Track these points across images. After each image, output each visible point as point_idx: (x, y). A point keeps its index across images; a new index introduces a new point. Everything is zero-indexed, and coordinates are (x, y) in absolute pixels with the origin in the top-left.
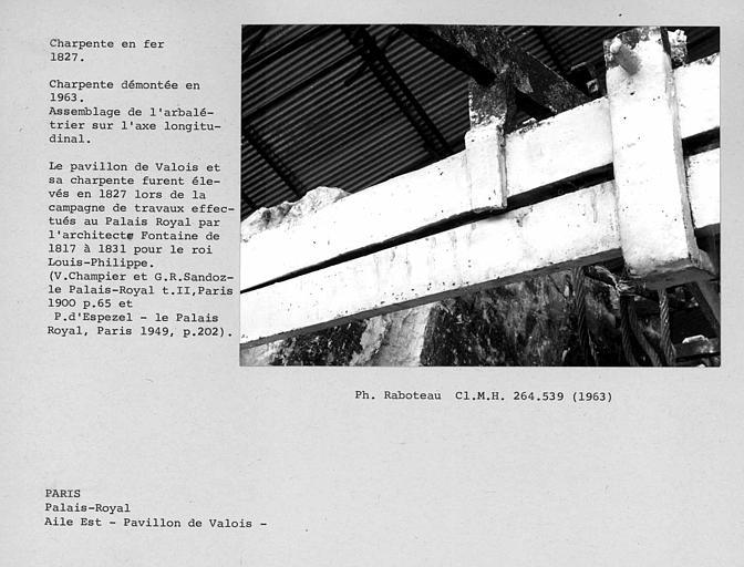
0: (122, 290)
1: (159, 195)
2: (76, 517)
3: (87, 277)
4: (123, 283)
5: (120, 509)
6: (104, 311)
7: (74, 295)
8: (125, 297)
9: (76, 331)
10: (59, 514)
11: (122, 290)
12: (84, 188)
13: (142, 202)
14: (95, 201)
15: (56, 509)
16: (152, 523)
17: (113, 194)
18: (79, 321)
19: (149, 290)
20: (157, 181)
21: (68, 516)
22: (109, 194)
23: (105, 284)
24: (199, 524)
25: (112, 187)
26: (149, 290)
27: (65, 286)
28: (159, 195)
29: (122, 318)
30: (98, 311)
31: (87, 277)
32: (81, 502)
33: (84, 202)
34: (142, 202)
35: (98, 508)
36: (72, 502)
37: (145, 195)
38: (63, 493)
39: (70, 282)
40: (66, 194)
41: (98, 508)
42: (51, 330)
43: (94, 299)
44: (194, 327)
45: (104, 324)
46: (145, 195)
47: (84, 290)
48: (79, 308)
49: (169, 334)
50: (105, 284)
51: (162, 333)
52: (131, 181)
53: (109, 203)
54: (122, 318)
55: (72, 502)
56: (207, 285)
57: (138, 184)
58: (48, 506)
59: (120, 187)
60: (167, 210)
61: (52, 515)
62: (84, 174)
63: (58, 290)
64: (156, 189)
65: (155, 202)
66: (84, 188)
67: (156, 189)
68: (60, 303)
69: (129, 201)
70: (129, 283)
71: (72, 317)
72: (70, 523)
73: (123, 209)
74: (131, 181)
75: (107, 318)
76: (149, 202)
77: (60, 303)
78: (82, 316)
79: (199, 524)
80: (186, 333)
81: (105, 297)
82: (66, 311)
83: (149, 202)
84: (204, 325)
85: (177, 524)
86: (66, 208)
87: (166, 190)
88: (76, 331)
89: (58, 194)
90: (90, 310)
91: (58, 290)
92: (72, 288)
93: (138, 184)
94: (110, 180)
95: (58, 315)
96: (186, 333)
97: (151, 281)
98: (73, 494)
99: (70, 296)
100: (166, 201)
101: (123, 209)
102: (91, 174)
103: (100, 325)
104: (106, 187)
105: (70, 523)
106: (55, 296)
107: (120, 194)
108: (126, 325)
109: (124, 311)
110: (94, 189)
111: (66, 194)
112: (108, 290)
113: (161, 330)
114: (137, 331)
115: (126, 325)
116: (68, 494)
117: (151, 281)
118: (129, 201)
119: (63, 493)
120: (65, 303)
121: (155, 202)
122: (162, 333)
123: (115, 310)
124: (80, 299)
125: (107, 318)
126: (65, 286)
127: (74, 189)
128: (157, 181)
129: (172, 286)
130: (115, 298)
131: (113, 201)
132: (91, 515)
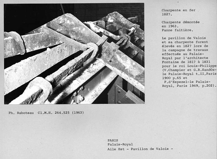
0: (184, 74)
1: (201, 46)
2: (117, 147)
3: (174, 70)
4: (184, 72)
5: (130, 145)
6: (179, 80)
7: (170, 76)
8: (185, 76)
9: (171, 86)
10: (112, 147)
11: (184, 74)
12: (179, 44)
13: (196, 48)
14: (182, 48)
15: (111, 145)
16: (139, 149)
17: (187, 46)
18: (172, 83)
19: (192, 74)
20: (200, 42)
21: (114, 147)
22: (186, 46)
23: (179, 72)
24: (153, 149)
25: (187, 44)
26: (192, 74)
27: (167, 73)
28: (201, 46)
29: (184, 82)
30: (177, 80)
31: (174, 70)
32: (118, 143)
33: (179, 48)
34: (196, 48)
35: (123, 144)
36: (116, 143)
37: (197, 46)
38: (113, 140)
39: (169, 72)
40: (174, 46)
41: (123, 144)
42: (163, 86)
43: (176, 77)
44: (205, 84)
45: (179, 84)
46: (197, 46)
47: (173, 74)
48: (171, 79)
49: (198, 86)
50: (179, 72)
51: (196, 86)
52: (192, 42)
53: (186, 49)
54: (184, 82)
55: (116, 143)
56: (209, 72)
57: (195, 43)
58: (109, 144)
59: (189, 44)
60: (203, 50)
61: (110, 147)
62: (179, 40)
63: (165, 74)
64: (200, 44)
65: (200, 48)
66: (179, 44)
67: (200, 44)
68: (166, 78)
69: (192, 48)
70: (186, 72)
71: (170, 82)
72: (115, 149)
73: (190, 50)
74: (192, 42)
75: (180, 82)
76: (198, 48)
77: (166, 78)
78: (173, 82)
79: (153, 149)
80: (203, 86)
81: (179, 76)
82: (168, 80)
83: (198, 48)
84: (208, 84)
85: (147, 149)
86: (174, 50)
87: (203, 45)
88: (171, 86)
89: (171, 46)
90: (175, 80)
91: (165, 74)
92: (169, 74)
93: (195, 43)
94: (187, 44)
95: (165, 82)
96: (203, 86)
97: (192, 71)
98: (116, 140)
99: (168, 76)
100: (203, 48)
101: (190, 50)
102: (181, 40)
103: (178, 84)
104: (185, 44)
105: (115, 149)
106: (164, 76)
107: (189, 46)
108: (185, 84)
109: (185, 80)
110: (182, 45)
111: (174, 46)
112: (180, 74)
113: (196, 85)
114: (189, 86)
115: (185, 84)
116: (114, 140)
117: (192, 71)
118: (192, 48)
119: (113, 140)
120: (167, 78)
121: (200, 48)
122: (196, 86)
123: (182, 80)
124: (172, 77)
125: (180, 82)
126: (167, 73)
127: (176, 45)
128: (200, 42)
129: (199, 72)
130: (182, 76)
131: (187, 48)
132: (121, 147)
